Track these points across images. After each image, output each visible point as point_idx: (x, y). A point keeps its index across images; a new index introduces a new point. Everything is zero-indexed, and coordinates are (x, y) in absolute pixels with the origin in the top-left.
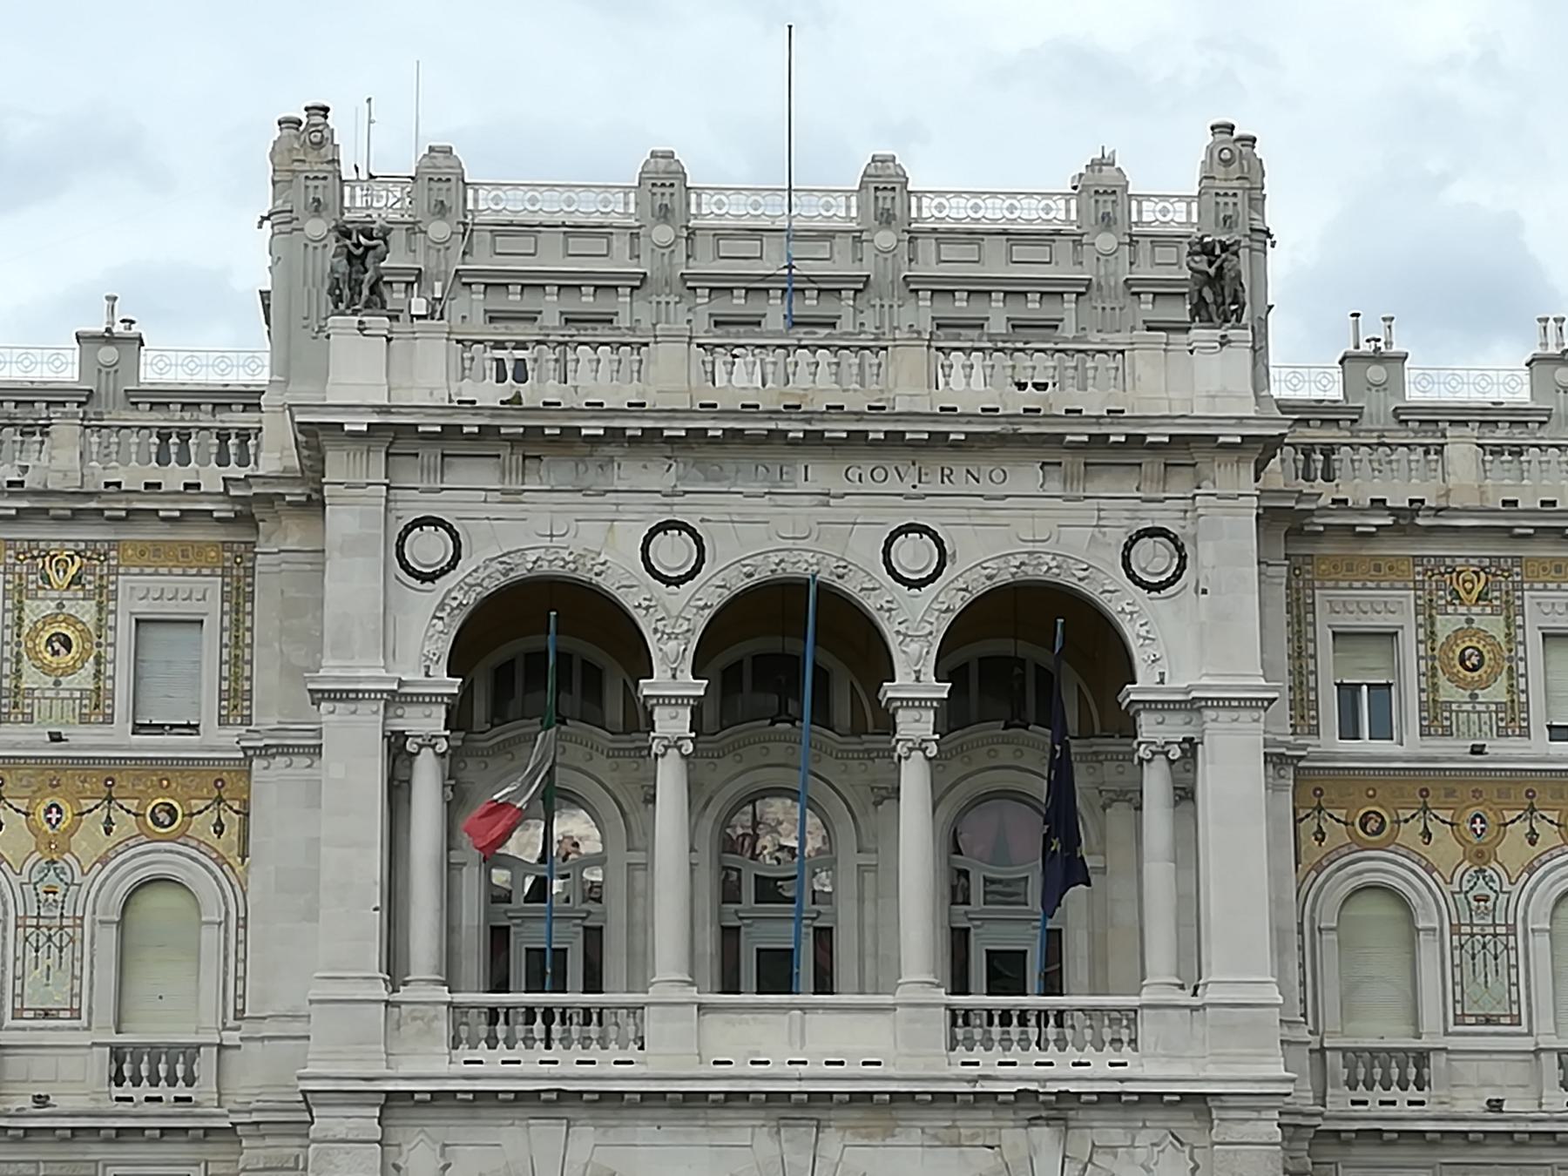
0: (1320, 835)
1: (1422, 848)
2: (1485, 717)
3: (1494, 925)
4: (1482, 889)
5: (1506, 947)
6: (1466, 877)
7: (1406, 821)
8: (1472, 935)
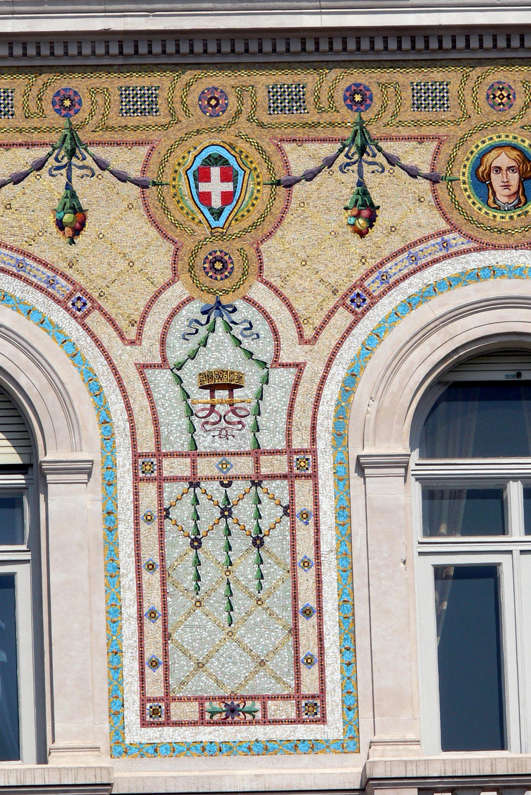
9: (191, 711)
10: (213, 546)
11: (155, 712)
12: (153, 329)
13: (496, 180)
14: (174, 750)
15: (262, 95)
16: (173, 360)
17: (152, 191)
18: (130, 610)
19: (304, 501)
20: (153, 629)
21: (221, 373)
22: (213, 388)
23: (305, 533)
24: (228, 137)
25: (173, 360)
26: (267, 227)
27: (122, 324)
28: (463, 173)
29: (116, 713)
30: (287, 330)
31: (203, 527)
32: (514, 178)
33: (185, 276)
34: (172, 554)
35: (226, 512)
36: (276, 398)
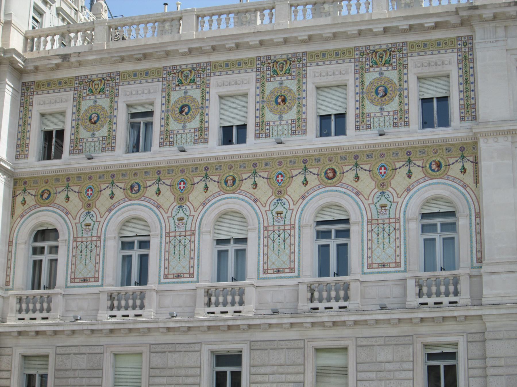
0: (24, 202)
1: (65, 204)
2: (97, 144)
3: (92, 236)
4: (88, 221)
5: (96, 246)
6: (82, 216)
7: (60, 193)
8: (82, 242)
9: (172, 276)
10: (177, 247)
11: (166, 276)
12: (170, 211)
13: (229, 182)
14: (169, 283)
15: (191, 169)
16: (173, 216)
17: (172, 187)
18: (163, 259)
19: (193, 239)
20: (167, 262)
21: (181, 218)
22: (179, 220)
23: (193, 245)
24: (185, 177)
25: (173, 216)
26: (190, 192)
27: (165, 210)
28: (223, 181)
29: (159, 277)
30: (192, 210)
31: (176, 244)
32: (232, 181)
33: (176, 201)
34: (171, 249)
35: (180, 242)
36: (189, 221)
